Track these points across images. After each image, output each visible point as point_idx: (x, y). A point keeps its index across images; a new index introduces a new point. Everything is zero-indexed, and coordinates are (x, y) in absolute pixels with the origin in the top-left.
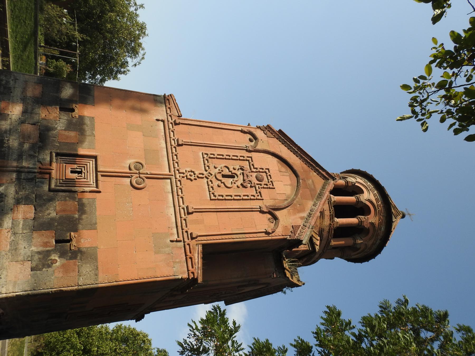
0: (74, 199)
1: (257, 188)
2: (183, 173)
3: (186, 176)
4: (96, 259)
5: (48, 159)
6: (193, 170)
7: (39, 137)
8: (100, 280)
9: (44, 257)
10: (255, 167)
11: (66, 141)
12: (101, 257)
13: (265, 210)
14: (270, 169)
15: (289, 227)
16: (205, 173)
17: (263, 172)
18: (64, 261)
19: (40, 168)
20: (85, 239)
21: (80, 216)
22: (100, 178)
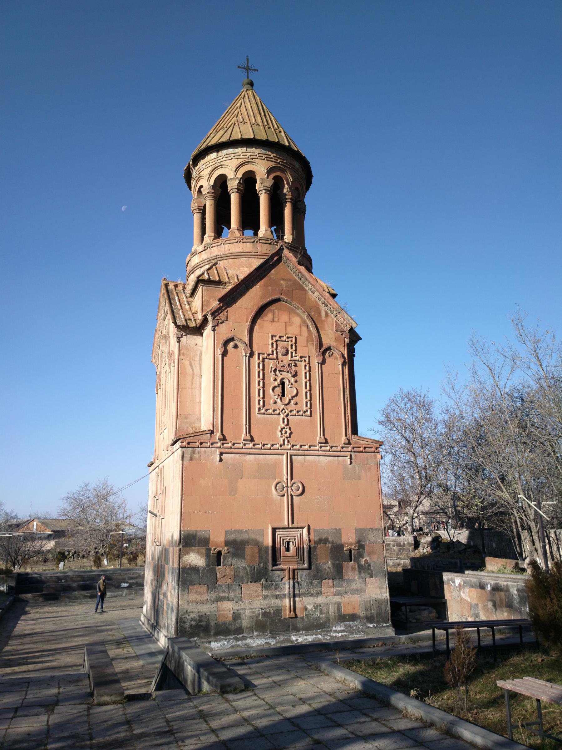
0: (315, 548)
1: (298, 358)
2: (284, 440)
3: (287, 438)
4: (364, 530)
5: (278, 572)
6: (280, 429)
7: (255, 582)
8: (377, 526)
10: (270, 352)
11: (258, 557)
12: (363, 526)
13: (321, 358)
14: (273, 334)
16: (282, 416)
17: (277, 345)
18: (366, 554)
19: (289, 579)
20: (349, 539)
21: (330, 543)
22: (295, 525)
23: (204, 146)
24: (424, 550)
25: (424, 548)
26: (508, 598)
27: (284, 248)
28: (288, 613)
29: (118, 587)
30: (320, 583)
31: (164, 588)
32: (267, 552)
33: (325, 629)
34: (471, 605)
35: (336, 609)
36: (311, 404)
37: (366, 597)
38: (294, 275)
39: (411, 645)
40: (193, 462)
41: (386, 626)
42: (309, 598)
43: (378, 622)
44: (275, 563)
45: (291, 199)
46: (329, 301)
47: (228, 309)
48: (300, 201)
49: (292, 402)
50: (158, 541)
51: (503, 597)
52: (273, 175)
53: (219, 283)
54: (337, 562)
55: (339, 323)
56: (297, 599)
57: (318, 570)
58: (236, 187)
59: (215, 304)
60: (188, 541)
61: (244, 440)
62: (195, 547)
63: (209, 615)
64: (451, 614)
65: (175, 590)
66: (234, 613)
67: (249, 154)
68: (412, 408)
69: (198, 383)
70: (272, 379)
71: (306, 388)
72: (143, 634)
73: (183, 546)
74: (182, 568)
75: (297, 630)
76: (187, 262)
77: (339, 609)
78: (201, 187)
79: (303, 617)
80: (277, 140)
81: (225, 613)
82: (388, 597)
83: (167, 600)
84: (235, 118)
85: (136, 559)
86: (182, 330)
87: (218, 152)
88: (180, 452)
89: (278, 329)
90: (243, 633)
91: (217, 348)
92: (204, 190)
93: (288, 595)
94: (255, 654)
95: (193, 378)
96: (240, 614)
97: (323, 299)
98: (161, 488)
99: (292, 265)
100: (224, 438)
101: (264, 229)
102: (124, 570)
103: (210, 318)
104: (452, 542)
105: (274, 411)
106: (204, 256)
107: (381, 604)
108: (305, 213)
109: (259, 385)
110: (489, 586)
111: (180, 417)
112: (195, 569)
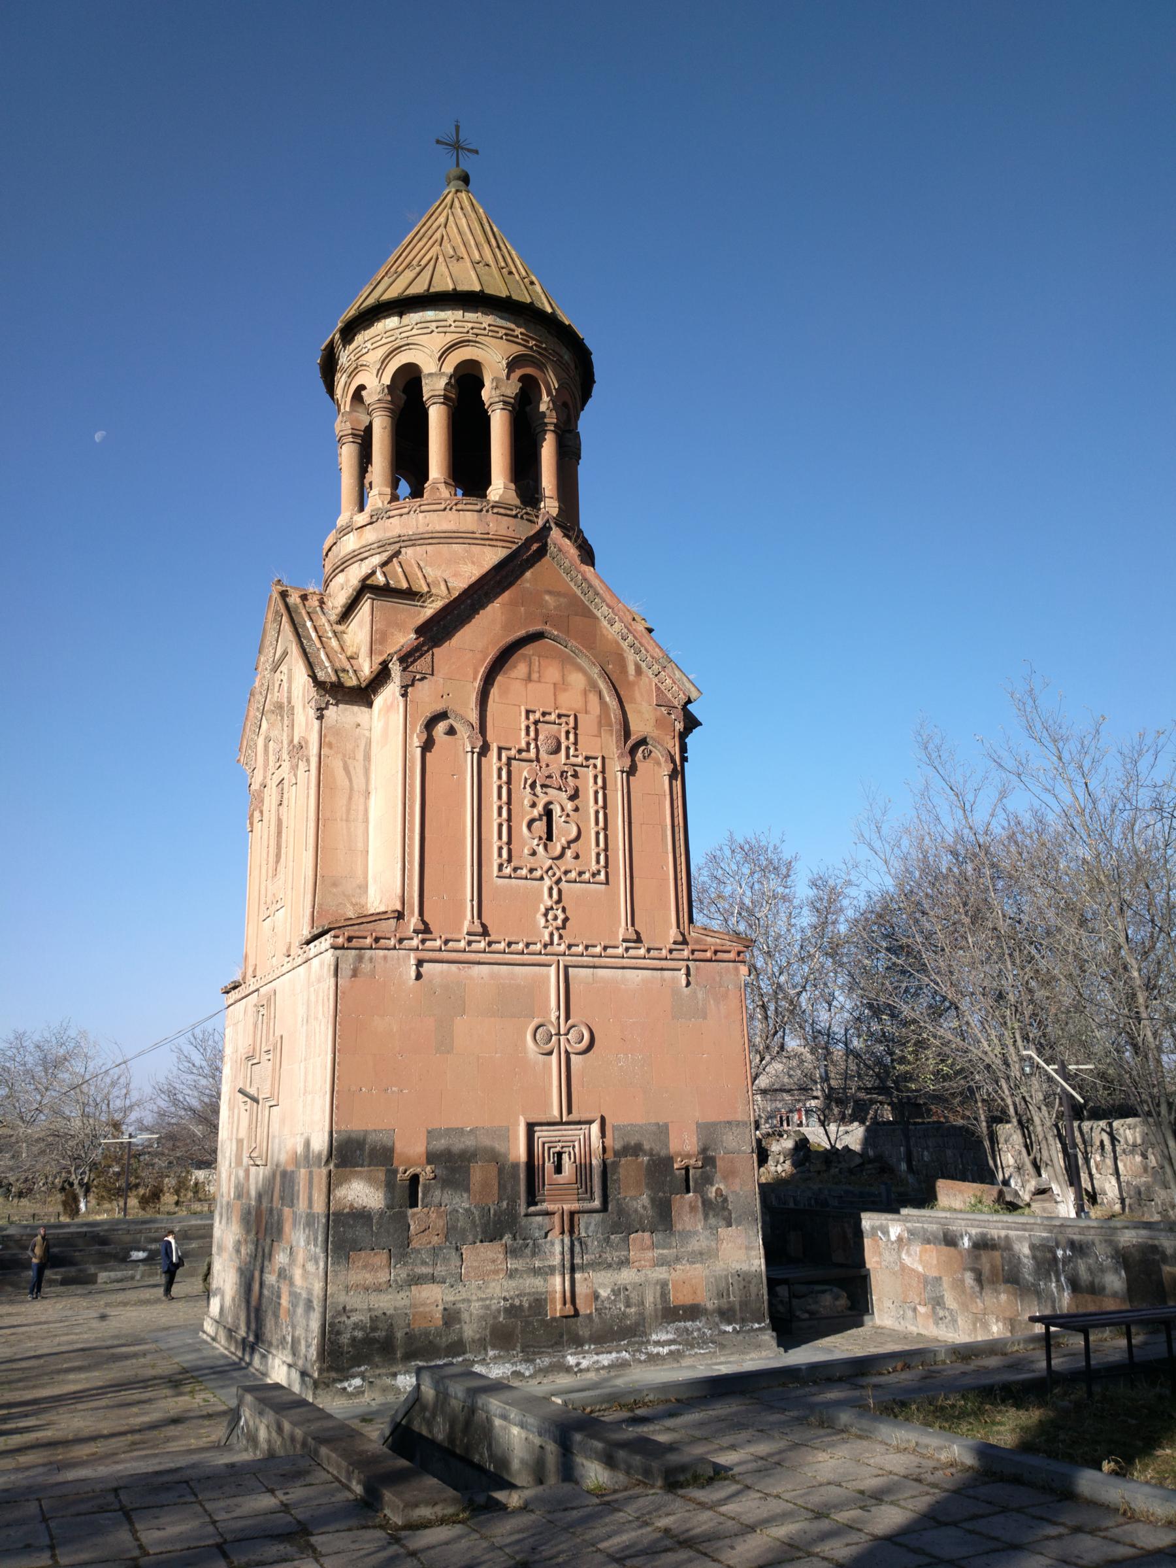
0: (616, 1164)
1: (580, 760)
2: (552, 935)
3: (558, 929)
4: (714, 1125)
5: (539, 1219)
6: (543, 910)
9: (714, 1209)
10: (523, 745)
11: (496, 1187)
12: (712, 1117)
13: (627, 762)
14: (529, 708)
15: (659, 713)
16: (547, 882)
19: (563, 1233)
20: (684, 1144)
21: (645, 1155)
23: (371, 301)
24: (779, 1167)
25: (778, 1162)
26: (1010, 1262)
27: (553, 526)
28: (559, 1307)
29: (123, 1258)
30: (626, 1240)
31: (281, 1258)
32: (515, 1176)
33: (637, 1339)
34: (925, 1281)
35: (658, 1295)
36: (607, 857)
37: (719, 1267)
38: (572, 584)
39: (961, 1367)
40: (360, 980)
41: (760, 1329)
42: (603, 1273)
43: (743, 1321)
44: (532, 1200)
45: (556, 425)
46: (644, 641)
47: (436, 650)
48: (570, 431)
49: (569, 853)
50: (260, 1156)
51: (998, 1262)
52: (518, 373)
53: (410, 594)
54: (661, 1194)
55: (663, 688)
56: (578, 1276)
57: (621, 1212)
58: (442, 393)
59: (405, 638)
60: (347, 1153)
61: (469, 934)
62: (362, 1166)
63: (391, 1317)
64: (879, 1299)
65: (317, 1263)
66: (445, 1309)
67: (470, 325)
68: (752, 873)
69: (361, 808)
70: (526, 802)
71: (597, 823)
72: (222, 1362)
73: (336, 1166)
74: (334, 1214)
75: (577, 1342)
76: (326, 547)
77: (664, 1295)
78: (362, 387)
79: (591, 1313)
80: (529, 301)
81: (427, 1309)
82: (763, 1267)
83: (292, 1284)
84: (436, 248)
85: (159, 1198)
86: (327, 692)
87: (401, 315)
88: (329, 957)
89: (539, 696)
90: (464, 1354)
91: (412, 733)
92: (370, 395)
93: (559, 1268)
94: (651, 1397)
95: (350, 798)
96: (459, 1312)
97: (631, 637)
98: (267, 1040)
99: (567, 564)
100: (427, 930)
101: (499, 486)
102: (134, 1222)
103: (395, 668)
104: (834, 1151)
105: (531, 871)
106: (370, 535)
107: (750, 1282)
108: (578, 457)
109: (500, 814)
110: (966, 1240)
111: (323, 881)
112: (361, 1216)
